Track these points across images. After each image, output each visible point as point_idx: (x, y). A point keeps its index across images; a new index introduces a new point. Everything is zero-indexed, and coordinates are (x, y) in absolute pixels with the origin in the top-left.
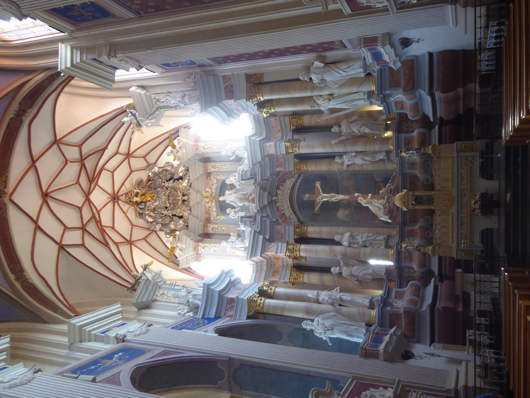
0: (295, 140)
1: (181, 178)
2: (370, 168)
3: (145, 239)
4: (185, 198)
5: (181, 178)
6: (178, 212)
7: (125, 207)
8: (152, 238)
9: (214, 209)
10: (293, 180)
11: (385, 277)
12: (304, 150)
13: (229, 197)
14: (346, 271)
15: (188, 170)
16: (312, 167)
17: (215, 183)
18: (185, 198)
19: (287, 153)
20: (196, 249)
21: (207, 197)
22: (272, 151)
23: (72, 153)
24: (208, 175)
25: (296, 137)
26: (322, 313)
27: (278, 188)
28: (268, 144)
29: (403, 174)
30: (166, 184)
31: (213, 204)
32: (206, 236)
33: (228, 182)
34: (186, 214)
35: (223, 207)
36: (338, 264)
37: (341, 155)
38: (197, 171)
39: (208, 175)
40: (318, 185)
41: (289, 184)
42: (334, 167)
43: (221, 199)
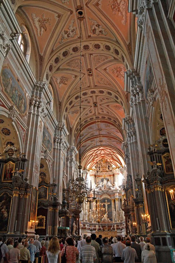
0: (118, 200)
1: (109, 169)
2: (113, 217)
3: (94, 163)
4: (104, 170)
5: (109, 169)
6: (101, 168)
7: (101, 158)
8: (94, 164)
9: (102, 178)
10: (110, 198)
11: (90, 221)
12: (117, 202)
13: (105, 181)
14: (90, 213)
15: (111, 171)
16: (113, 203)
17: (109, 178)
18: (104, 170)
19: (115, 198)
20: (92, 175)
21: (105, 176)
22: (116, 195)
23: (112, 153)
24: (110, 176)
25: (119, 199)
26: (84, 211)
27: (108, 194)
28: (117, 194)
29: (112, 224)
30: (107, 165)
31: (103, 178)
32: (95, 176)
33: (109, 182)
34: (100, 171)
35: (102, 181)
36: (92, 211)
37: (115, 210)
38: (111, 173)
39: (110, 176)
40: (109, 203)
41: (109, 197)
42: (113, 209)
43: (105, 180)
